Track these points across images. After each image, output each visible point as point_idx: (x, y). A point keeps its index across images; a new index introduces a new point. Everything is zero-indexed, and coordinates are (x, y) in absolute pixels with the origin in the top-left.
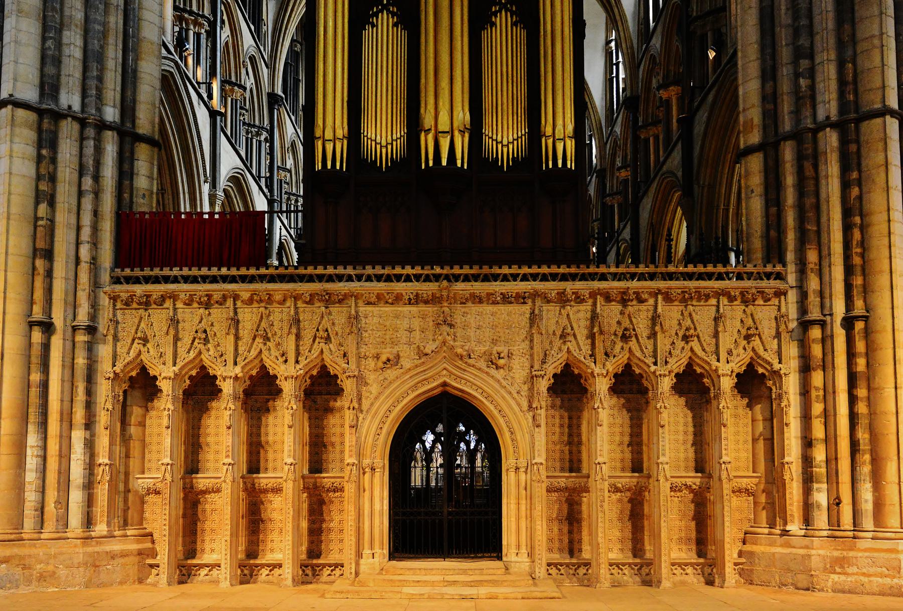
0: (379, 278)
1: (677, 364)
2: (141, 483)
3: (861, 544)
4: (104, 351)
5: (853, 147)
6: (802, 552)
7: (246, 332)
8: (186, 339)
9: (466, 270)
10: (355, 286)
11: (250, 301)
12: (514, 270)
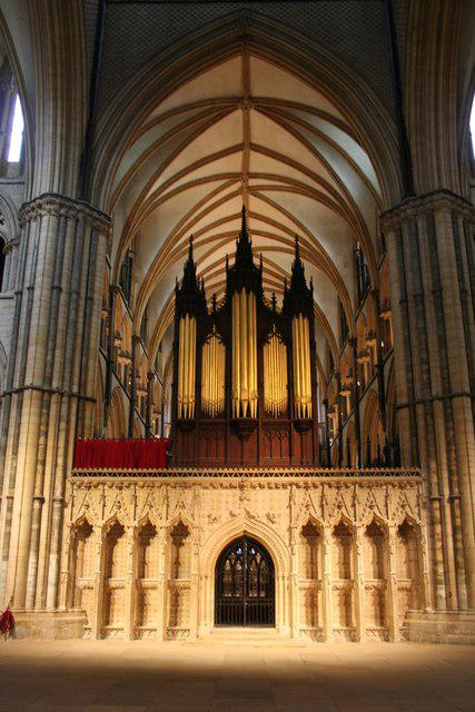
0: (210, 475)
1: (367, 521)
3: (462, 618)
4: (67, 511)
5: (449, 410)
6: (432, 622)
8: (109, 505)
9: (256, 471)
10: (198, 479)
11: (143, 487)
12: (281, 471)
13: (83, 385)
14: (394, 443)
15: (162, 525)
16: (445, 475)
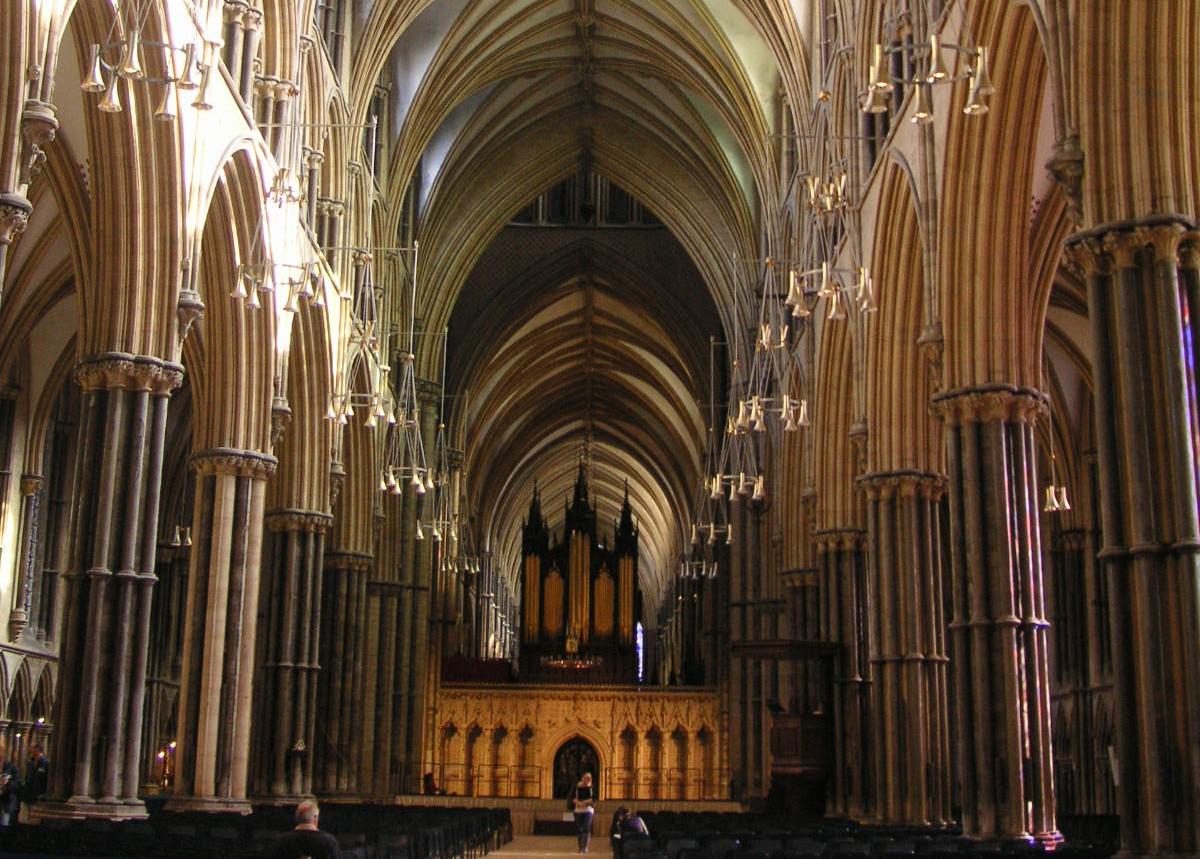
1: (672, 728)
4: (438, 717)
7: (495, 709)
10: (540, 692)
15: (513, 728)
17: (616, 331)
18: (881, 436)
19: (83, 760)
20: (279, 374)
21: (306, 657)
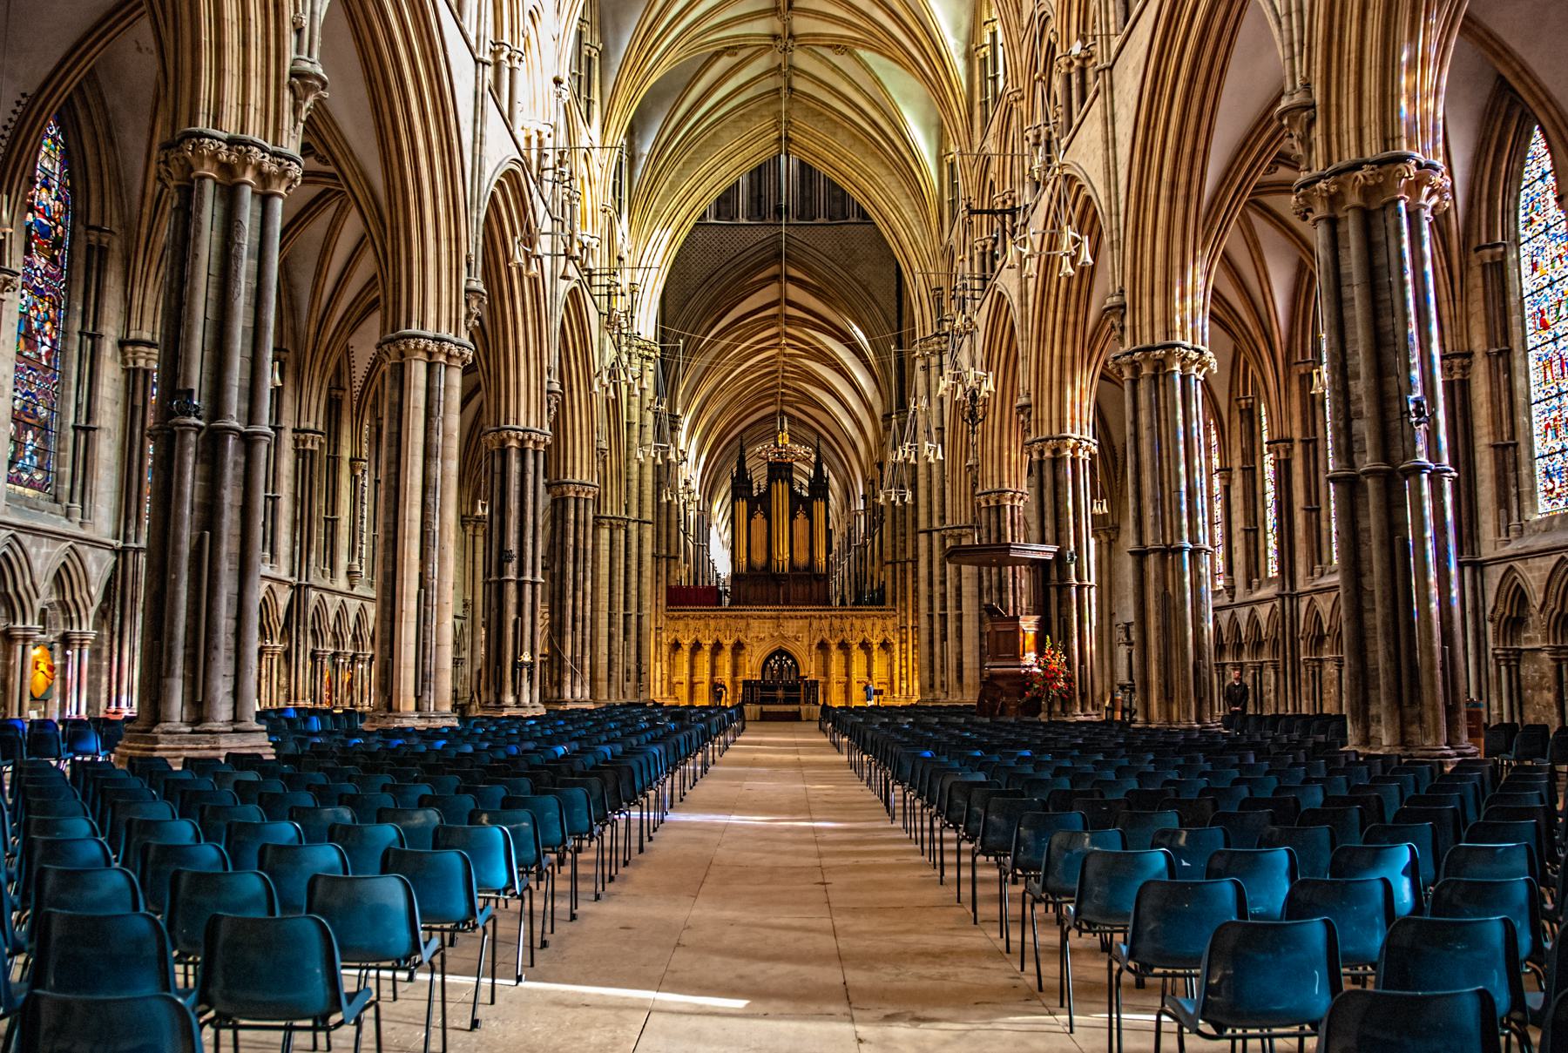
1: (859, 640)
2: (675, 680)
4: (664, 635)
13: (668, 549)
14: (882, 589)
16: (910, 611)
17: (804, 322)
18: (1140, 308)
19: (170, 673)
20: (472, 251)
21: (529, 572)
